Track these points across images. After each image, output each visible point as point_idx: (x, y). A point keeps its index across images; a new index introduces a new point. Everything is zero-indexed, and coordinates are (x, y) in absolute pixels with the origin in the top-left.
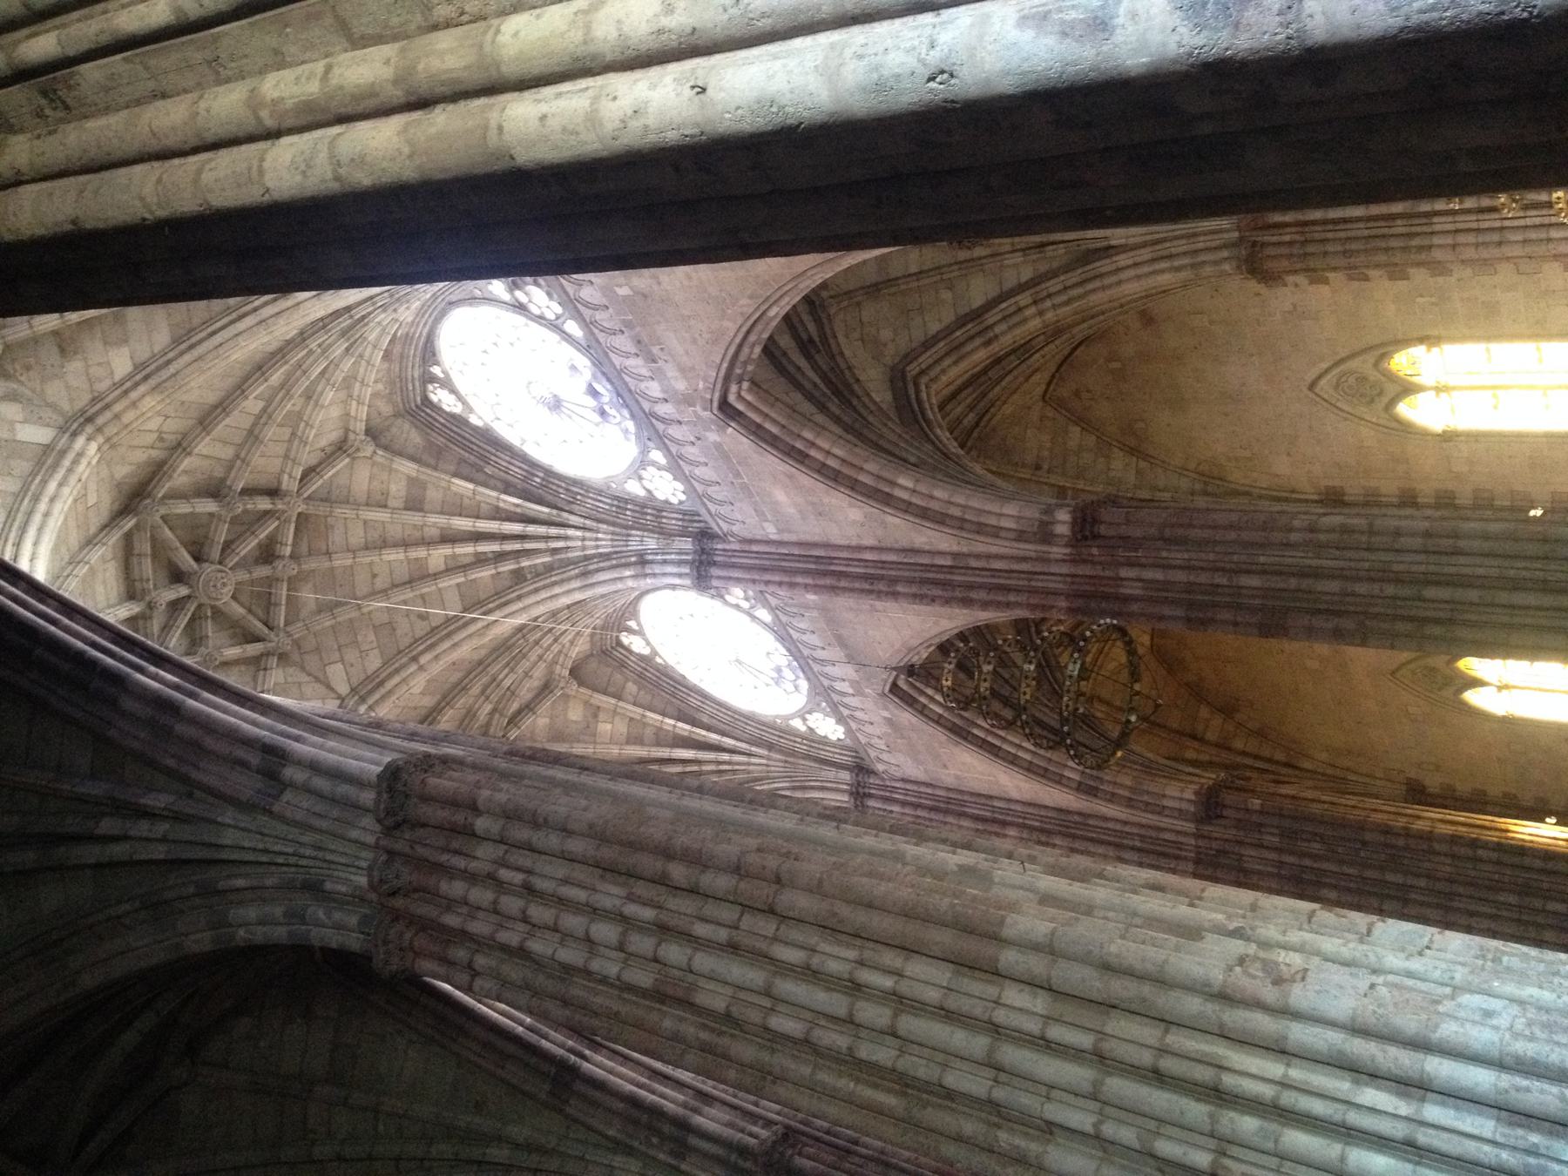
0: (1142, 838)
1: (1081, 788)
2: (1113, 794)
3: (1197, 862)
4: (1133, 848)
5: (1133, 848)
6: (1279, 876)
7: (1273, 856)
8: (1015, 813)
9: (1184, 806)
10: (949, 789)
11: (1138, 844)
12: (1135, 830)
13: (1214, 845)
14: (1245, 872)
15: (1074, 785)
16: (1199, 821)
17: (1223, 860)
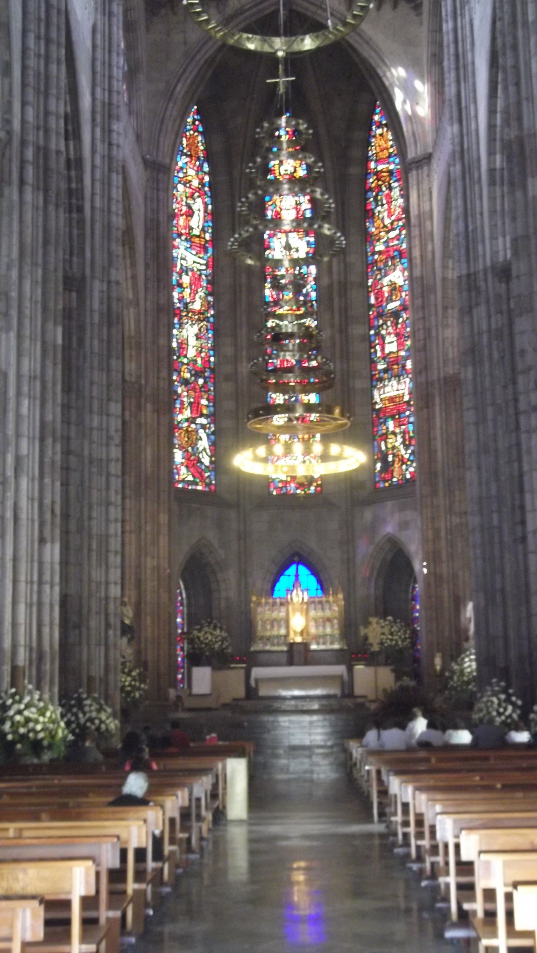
0: (474, 231)
1: (492, 171)
2: (495, 198)
3: (469, 275)
4: (467, 227)
5: (467, 227)
6: (472, 336)
7: (485, 327)
8: (469, 125)
9: (501, 254)
10: (473, 63)
11: (470, 228)
12: (479, 223)
13: (482, 284)
14: (470, 312)
15: (492, 166)
16: (493, 267)
17: (473, 294)
